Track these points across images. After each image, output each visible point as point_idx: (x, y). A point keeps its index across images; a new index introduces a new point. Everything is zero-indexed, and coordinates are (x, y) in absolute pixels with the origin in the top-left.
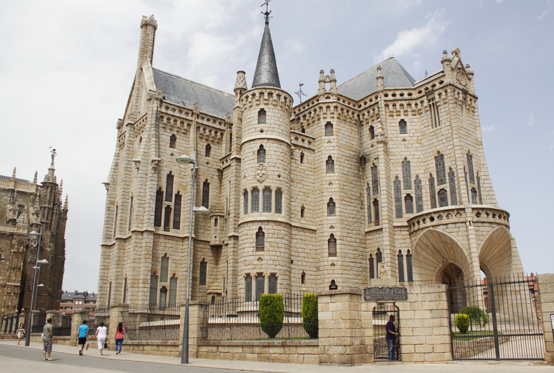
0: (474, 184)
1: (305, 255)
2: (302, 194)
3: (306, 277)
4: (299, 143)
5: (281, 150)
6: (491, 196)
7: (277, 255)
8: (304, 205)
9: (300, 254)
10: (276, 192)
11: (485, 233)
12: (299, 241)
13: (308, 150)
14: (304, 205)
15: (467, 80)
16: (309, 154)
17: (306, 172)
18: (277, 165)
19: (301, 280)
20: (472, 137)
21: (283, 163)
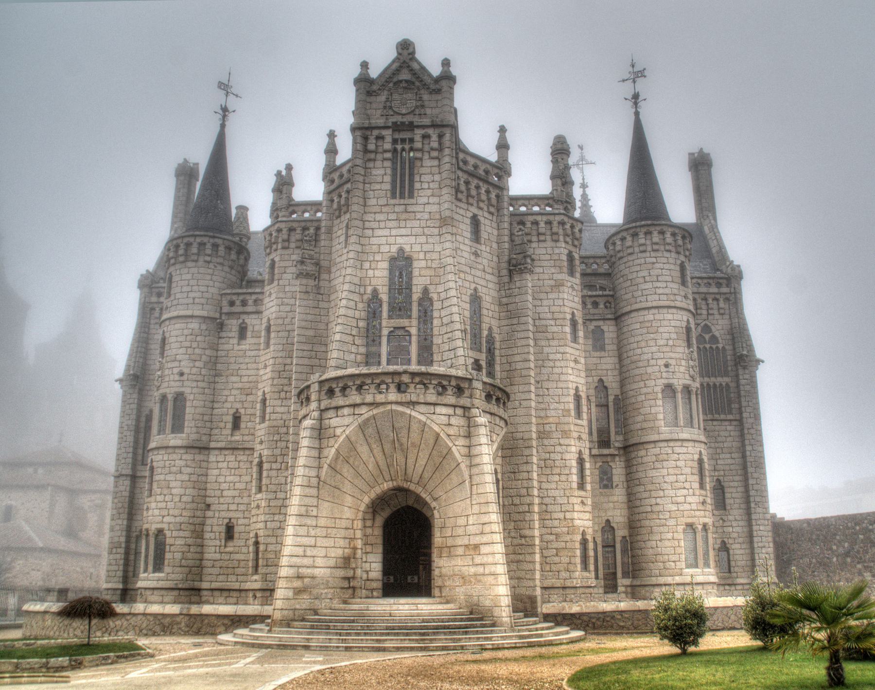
0: (410, 317)
1: (236, 493)
2: (238, 392)
3: (237, 529)
4: (237, 309)
5: (186, 332)
6: (450, 335)
7: (166, 500)
8: (242, 411)
9: (225, 493)
10: (175, 400)
11: (338, 431)
12: (224, 472)
13: (253, 316)
14: (239, 410)
15: (426, 97)
16: (255, 322)
17: (249, 353)
18: (178, 356)
19: (223, 535)
20: (418, 216)
21: (190, 351)
